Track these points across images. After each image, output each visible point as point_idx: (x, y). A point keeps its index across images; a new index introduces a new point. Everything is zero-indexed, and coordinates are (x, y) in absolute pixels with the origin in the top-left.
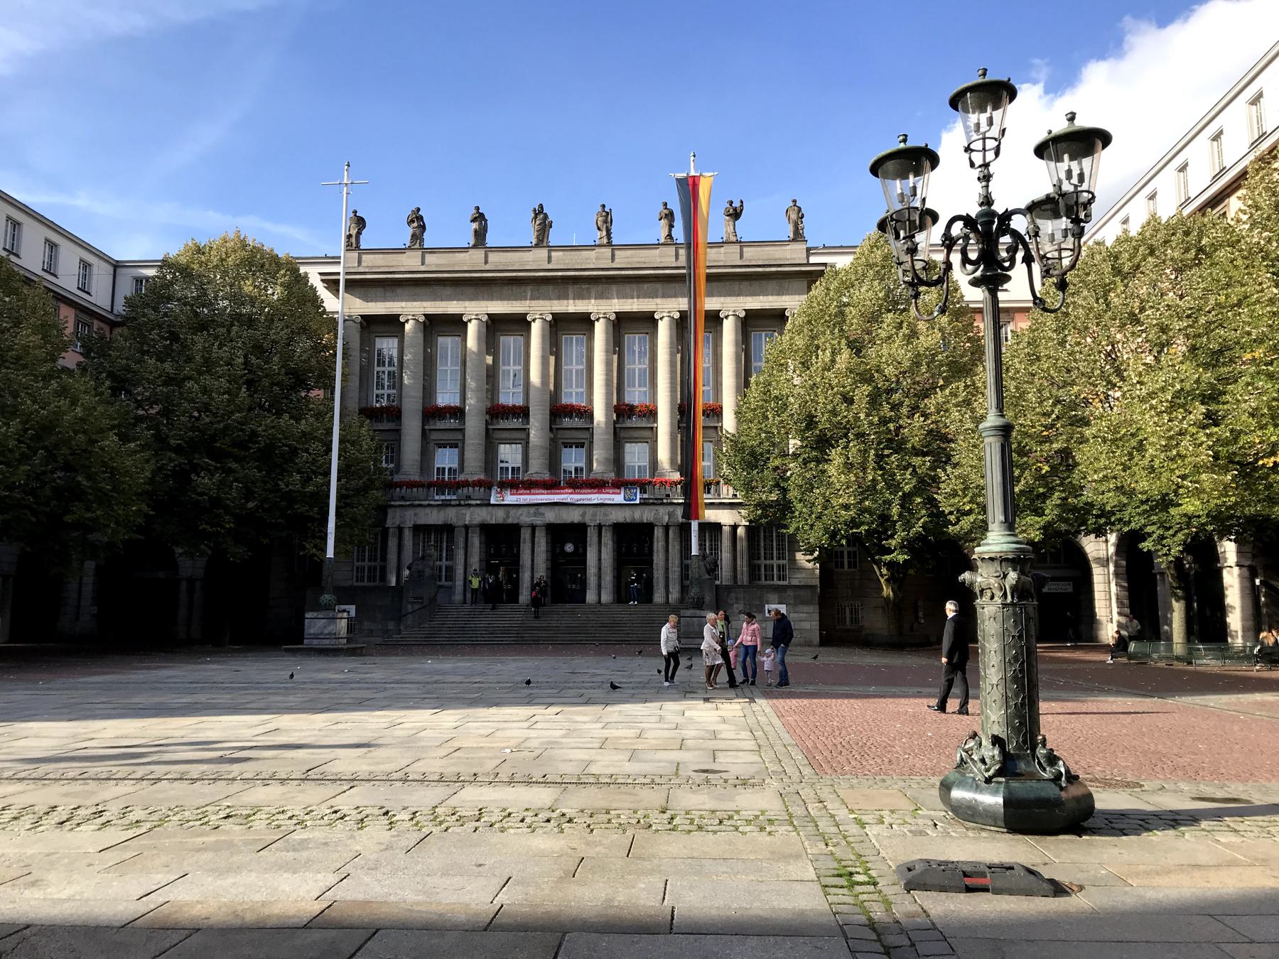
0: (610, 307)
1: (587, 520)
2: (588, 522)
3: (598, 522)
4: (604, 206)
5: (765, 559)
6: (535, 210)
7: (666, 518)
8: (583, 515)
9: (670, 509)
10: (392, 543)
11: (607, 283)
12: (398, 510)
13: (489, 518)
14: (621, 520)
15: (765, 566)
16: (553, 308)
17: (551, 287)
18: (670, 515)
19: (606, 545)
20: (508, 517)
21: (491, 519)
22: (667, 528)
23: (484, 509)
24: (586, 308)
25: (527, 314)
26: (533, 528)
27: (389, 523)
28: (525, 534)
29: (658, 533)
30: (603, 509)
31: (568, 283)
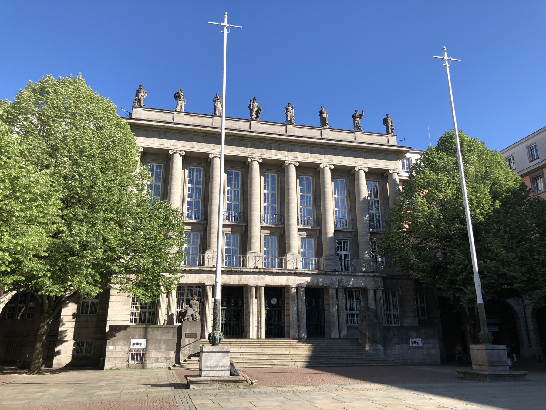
0: (295, 159)
5: (393, 311)
8: (288, 280)
15: (394, 315)
16: (263, 156)
18: (340, 282)
21: (230, 281)
22: (337, 290)
24: (282, 157)
25: (248, 157)
26: (257, 288)
29: (332, 292)
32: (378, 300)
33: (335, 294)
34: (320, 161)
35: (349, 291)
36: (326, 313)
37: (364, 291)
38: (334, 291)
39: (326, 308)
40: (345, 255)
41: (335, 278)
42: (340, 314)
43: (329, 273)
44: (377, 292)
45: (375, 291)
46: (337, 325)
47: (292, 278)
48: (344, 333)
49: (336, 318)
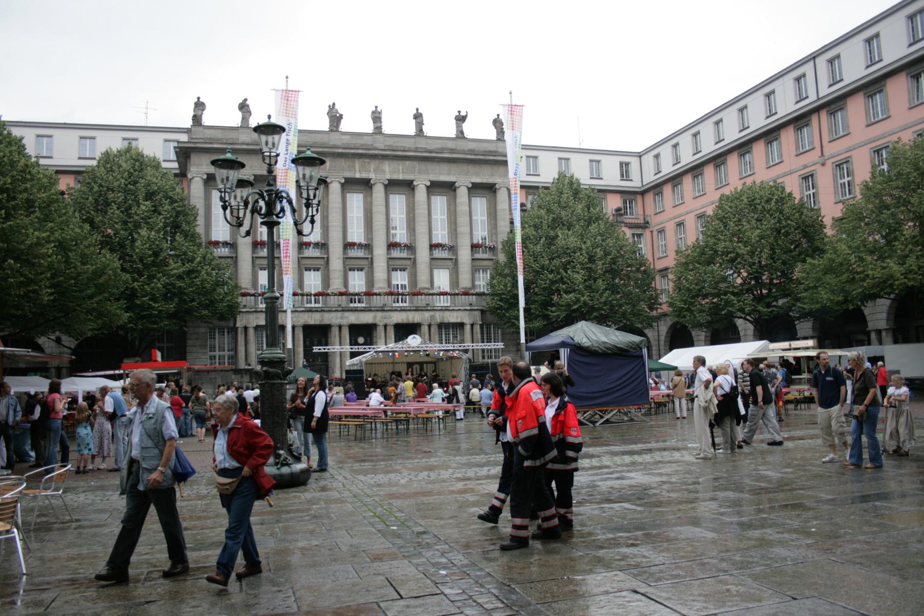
1: (377, 321)
2: (378, 323)
4: (376, 107)
6: (329, 106)
8: (375, 318)
9: (431, 313)
10: (241, 338)
11: (382, 159)
12: (244, 315)
13: (309, 320)
14: (400, 321)
17: (343, 160)
19: (390, 338)
20: (323, 319)
22: (430, 326)
23: (306, 314)
26: (340, 327)
27: (238, 324)
28: (335, 331)
31: (356, 158)
32: (475, 335)
41: (427, 315)
44: (475, 327)
45: (472, 325)
47: (380, 314)
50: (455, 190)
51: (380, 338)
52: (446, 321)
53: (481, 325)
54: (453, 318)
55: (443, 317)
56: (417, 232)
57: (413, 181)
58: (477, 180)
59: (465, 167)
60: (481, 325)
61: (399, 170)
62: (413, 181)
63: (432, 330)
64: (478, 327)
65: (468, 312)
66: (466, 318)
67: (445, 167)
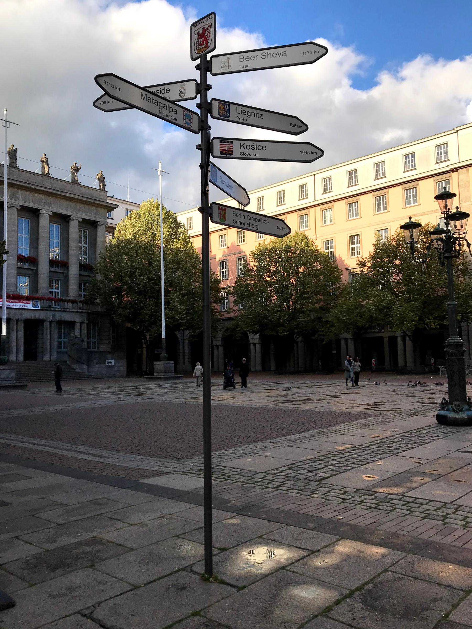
3: (17, 318)
7: (51, 318)
9: (53, 313)
18: (53, 316)
22: (51, 323)
29: (47, 325)
30: (20, 311)
33: (48, 326)
34: (40, 207)
35: (60, 323)
36: (40, 341)
37: (71, 324)
38: (48, 324)
39: (40, 336)
40: (55, 292)
42: (52, 342)
43: (46, 309)
45: (81, 324)
46: (49, 350)
48: (54, 356)
49: (48, 345)
50: (68, 222)
51: (13, 330)
52: (63, 319)
53: (87, 324)
54: (67, 317)
55: (61, 316)
56: (40, 250)
57: (40, 210)
58: (86, 217)
59: (78, 206)
60: (87, 324)
61: (29, 200)
62: (40, 210)
63: (53, 325)
64: (85, 325)
65: (79, 314)
66: (77, 319)
67: (64, 203)
